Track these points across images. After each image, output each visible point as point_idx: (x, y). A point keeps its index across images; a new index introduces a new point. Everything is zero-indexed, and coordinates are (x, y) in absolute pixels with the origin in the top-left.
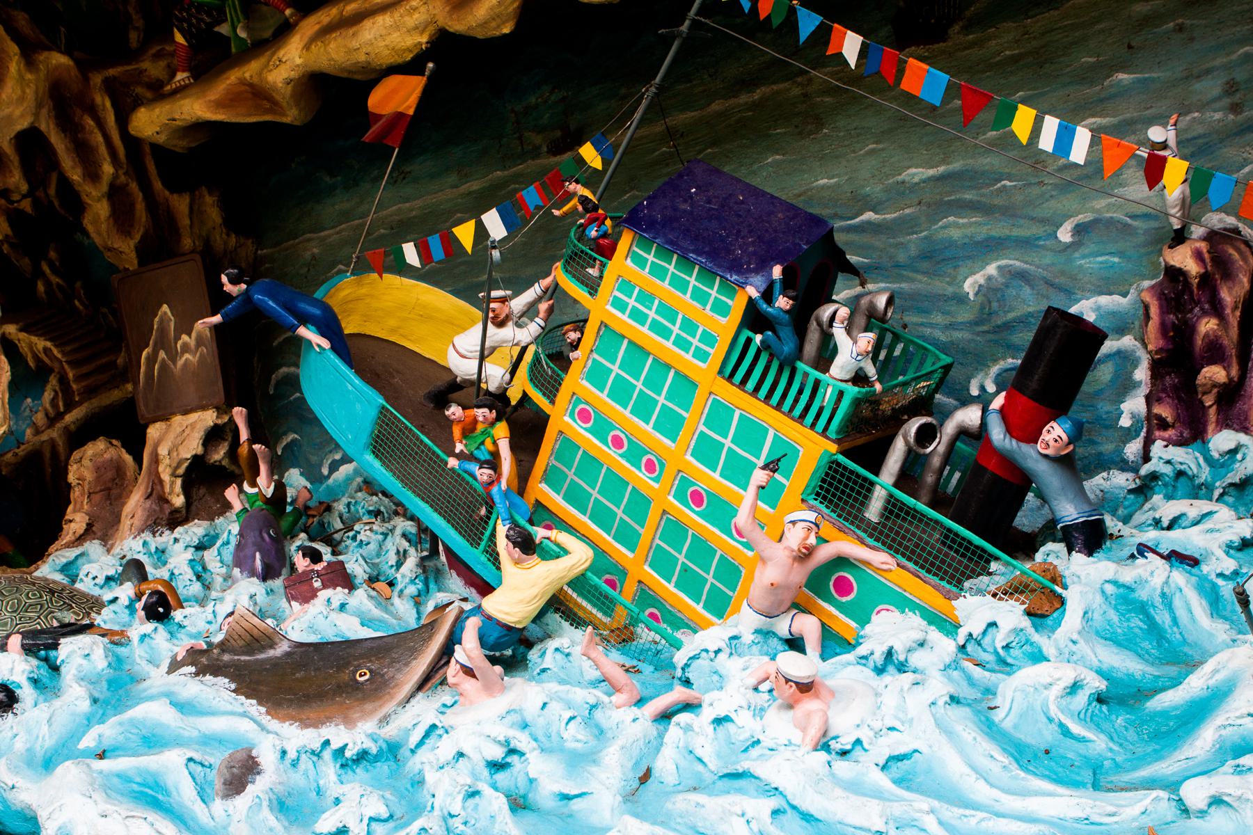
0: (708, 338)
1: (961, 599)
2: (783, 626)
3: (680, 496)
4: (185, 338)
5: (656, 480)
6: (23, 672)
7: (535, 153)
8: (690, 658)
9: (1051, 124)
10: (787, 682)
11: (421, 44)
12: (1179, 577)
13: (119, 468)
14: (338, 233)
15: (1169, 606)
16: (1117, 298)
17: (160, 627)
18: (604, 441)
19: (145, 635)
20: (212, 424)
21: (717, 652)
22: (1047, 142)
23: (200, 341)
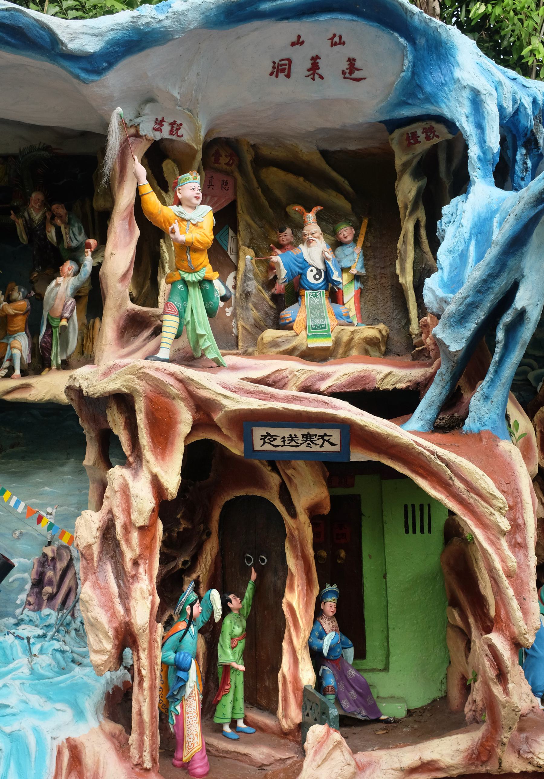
12: (17, 642)
15: (12, 650)
16: (26, 560)
22: (12, 504)
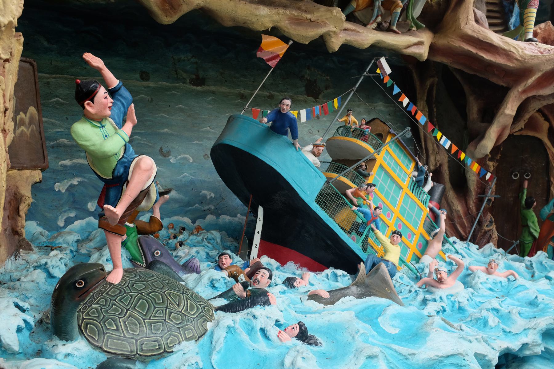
4: (22, 114)
9: (444, 138)
14: (54, 78)
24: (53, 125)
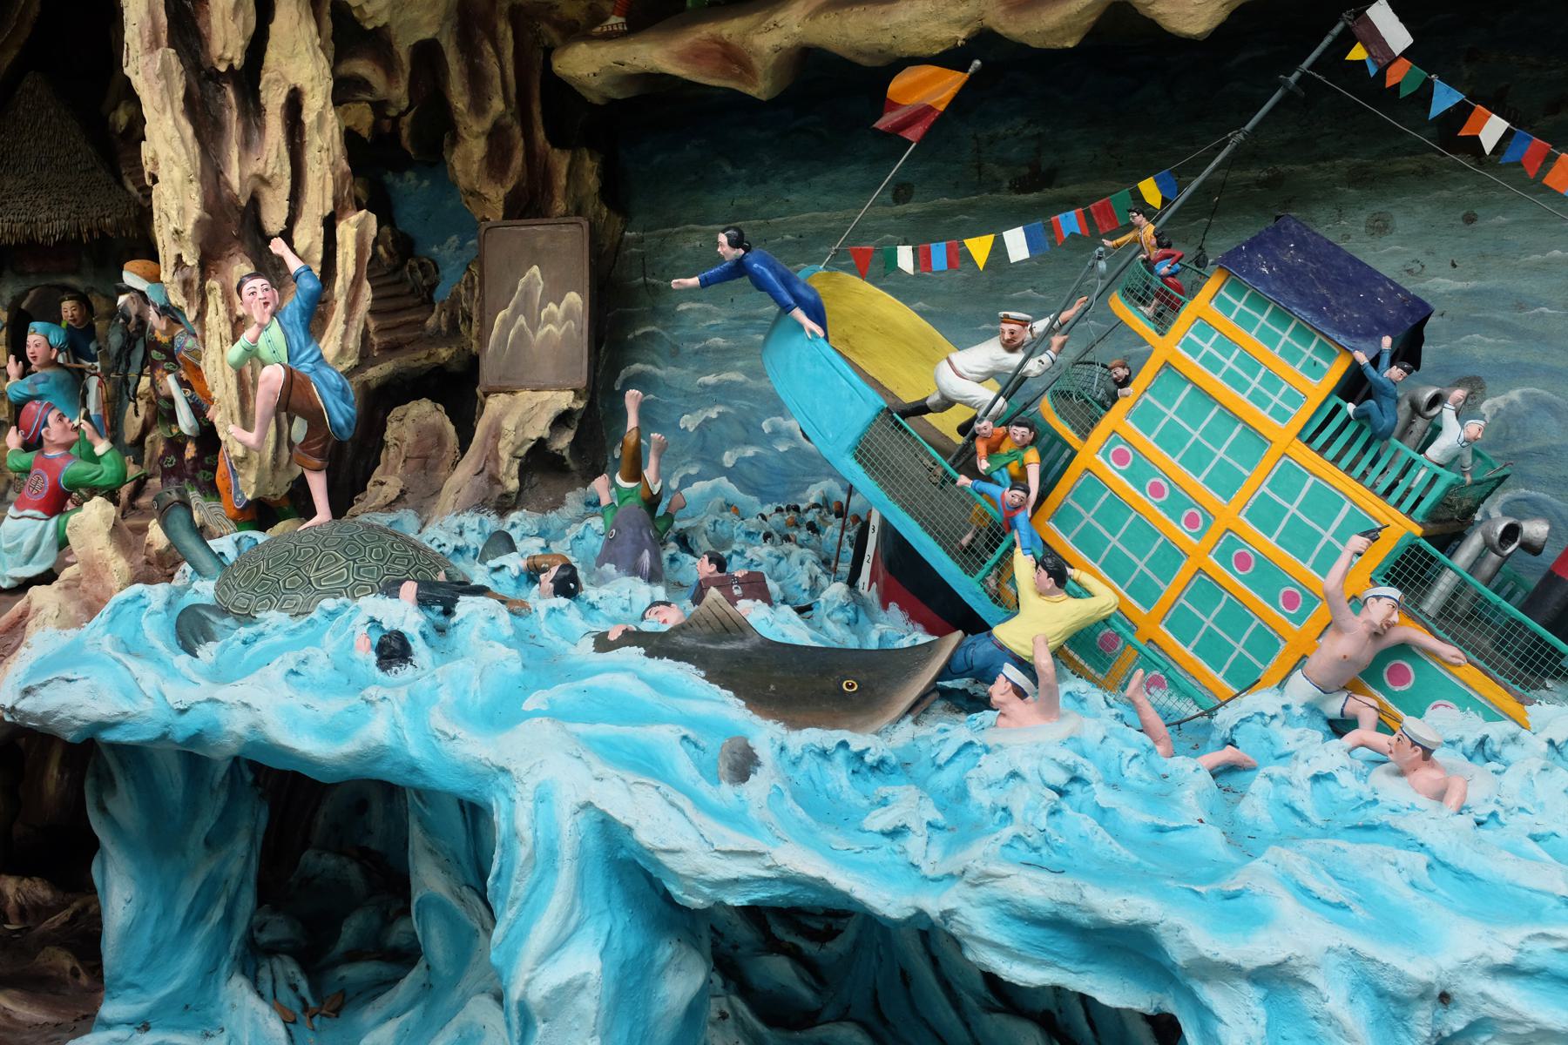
0: (1294, 398)
1: (1536, 705)
2: (1334, 707)
3: (1223, 557)
4: (552, 306)
5: (1198, 536)
6: (416, 623)
7: (995, 187)
8: (1242, 720)
10: (1412, 746)
11: (957, 39)
13: (440, 440)
17: (573, 605)
18: (1141, 487)
19: (554, 609)
20: (566, 407)
21: (1273, 717)
23: (569, 314)
24: (708, 313)
